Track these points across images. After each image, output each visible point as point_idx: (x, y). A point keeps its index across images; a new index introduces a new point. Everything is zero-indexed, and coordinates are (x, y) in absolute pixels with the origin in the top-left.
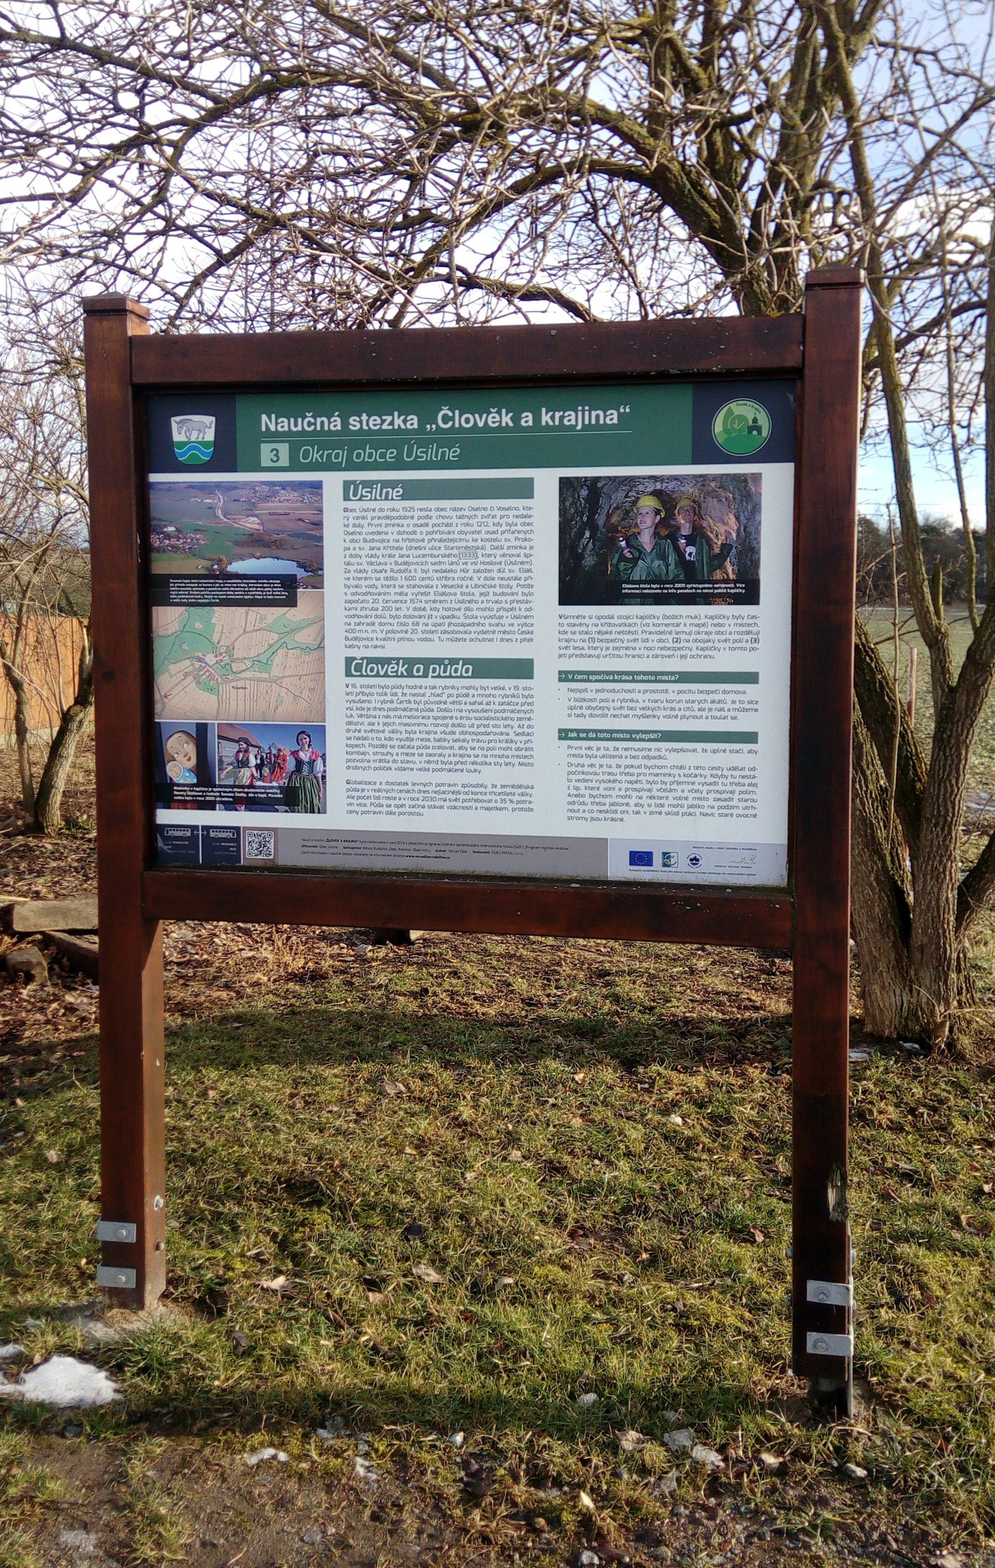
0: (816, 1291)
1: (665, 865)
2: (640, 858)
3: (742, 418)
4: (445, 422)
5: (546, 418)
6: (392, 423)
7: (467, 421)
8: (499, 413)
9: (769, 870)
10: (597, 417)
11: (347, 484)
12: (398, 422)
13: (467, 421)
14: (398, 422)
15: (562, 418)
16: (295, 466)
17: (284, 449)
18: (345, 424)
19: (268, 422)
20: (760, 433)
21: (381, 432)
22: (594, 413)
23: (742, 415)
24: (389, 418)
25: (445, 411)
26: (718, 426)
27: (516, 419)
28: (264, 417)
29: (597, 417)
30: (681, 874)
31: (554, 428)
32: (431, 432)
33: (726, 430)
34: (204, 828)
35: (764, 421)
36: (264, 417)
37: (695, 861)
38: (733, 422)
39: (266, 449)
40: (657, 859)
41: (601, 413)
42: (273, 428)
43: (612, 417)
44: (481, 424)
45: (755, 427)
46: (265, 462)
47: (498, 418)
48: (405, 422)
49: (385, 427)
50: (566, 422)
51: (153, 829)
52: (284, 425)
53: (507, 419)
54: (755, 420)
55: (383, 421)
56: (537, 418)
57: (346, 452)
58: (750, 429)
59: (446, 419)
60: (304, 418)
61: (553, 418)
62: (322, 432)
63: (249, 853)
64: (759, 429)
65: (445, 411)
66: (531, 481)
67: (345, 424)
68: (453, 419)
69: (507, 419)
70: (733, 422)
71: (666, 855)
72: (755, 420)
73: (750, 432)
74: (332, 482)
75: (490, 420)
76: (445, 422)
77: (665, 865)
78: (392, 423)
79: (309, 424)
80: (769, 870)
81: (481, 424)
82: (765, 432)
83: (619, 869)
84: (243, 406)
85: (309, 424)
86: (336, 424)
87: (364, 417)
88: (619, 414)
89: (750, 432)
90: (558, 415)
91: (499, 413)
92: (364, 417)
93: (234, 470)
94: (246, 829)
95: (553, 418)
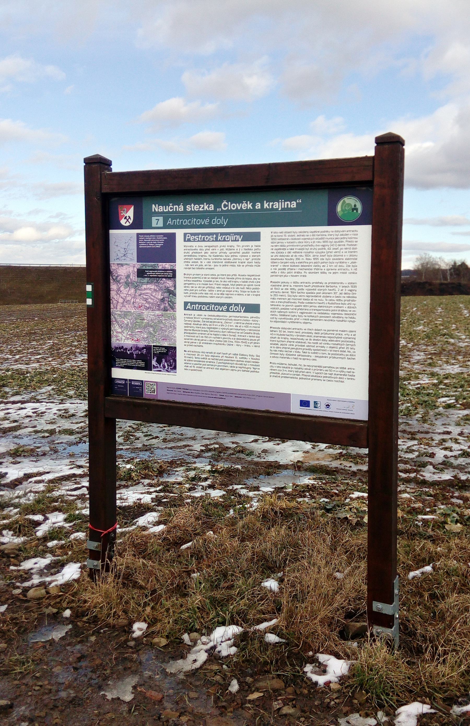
0: (378, 606)
1: (315, 407)
2: (305, 403)
3: (349, 205)
4: (225, 207)
5: (266, 205)
6: (203, 208)
7: (234, 207)
8: (247, 203)
9: (361, 413)
10: (288, 204)
11: (185, 234)
12: (206, 207)
13: (234, 207)
14: (206, 207)
15: (273, 205)
16: (165, 227)
17: (161, 219)
18: (185, 208)
19: (155, 208)
20: (357, 212)
21: (199, 212)
22: (286, 203)
23: (349, 203)
24: (202, 206)
25: (225, 202)
26: (339, 208)
27: (254, 206)
28: (153, 206)
29: (288, 204)
30: (321, 412)
31: (269, 210)
32: (219, 212)
33: (342, 210)
34: (131, 380)
35: (359, 206)
36: (153, 206)
37: (328, 406)
38: (345, 206)
39: (154, 219)
40: (312, 404)
41: (289, 203)
42: (157, 210)
43: (294, 205)
44: (239, 208)
45: (355, 209)
46: (154, 225)
47: (247, 205)
48: (209, 207)
49: (201, 209)
50: (274, 207)
51: (111, 381)
52: (161, 209)
53: (250, 206)
54: (355, 206)
55: (200, 207)
56: (262, 205)
57: (185, 221)
58: (353, 210)
59: (225, 206)
60: (169, 206)
61: (269, 205)
62: (176, 212)
63: (147, 393)
64: (357, 210)
65: (225, 202)
66: (259, 233)
67: (185, 208)
68: (228, 206)
69: (250, 206)
70: (345, 206)
71: (315, 403)
72: (355, 206)
73: (353, 211)
74: (179, 233)
75: (243, 206)
76: (225, 207)
77: (315, 407)
78: (203, 208)
79: (171, 208)
80: (361, 413)
81: (239, 208)
82: (360, 211)
83: (296, 409)
84: (145, 202)
85: (171, 208)
86: (181, 208)
87: (193, 205)
88: (297, 203)
89: (353, 211)
90: (271, 204)
91: (247, 203)
92: (193, 205)
93: (142, 229)
94: (145, 381)
95: (269, 205)
